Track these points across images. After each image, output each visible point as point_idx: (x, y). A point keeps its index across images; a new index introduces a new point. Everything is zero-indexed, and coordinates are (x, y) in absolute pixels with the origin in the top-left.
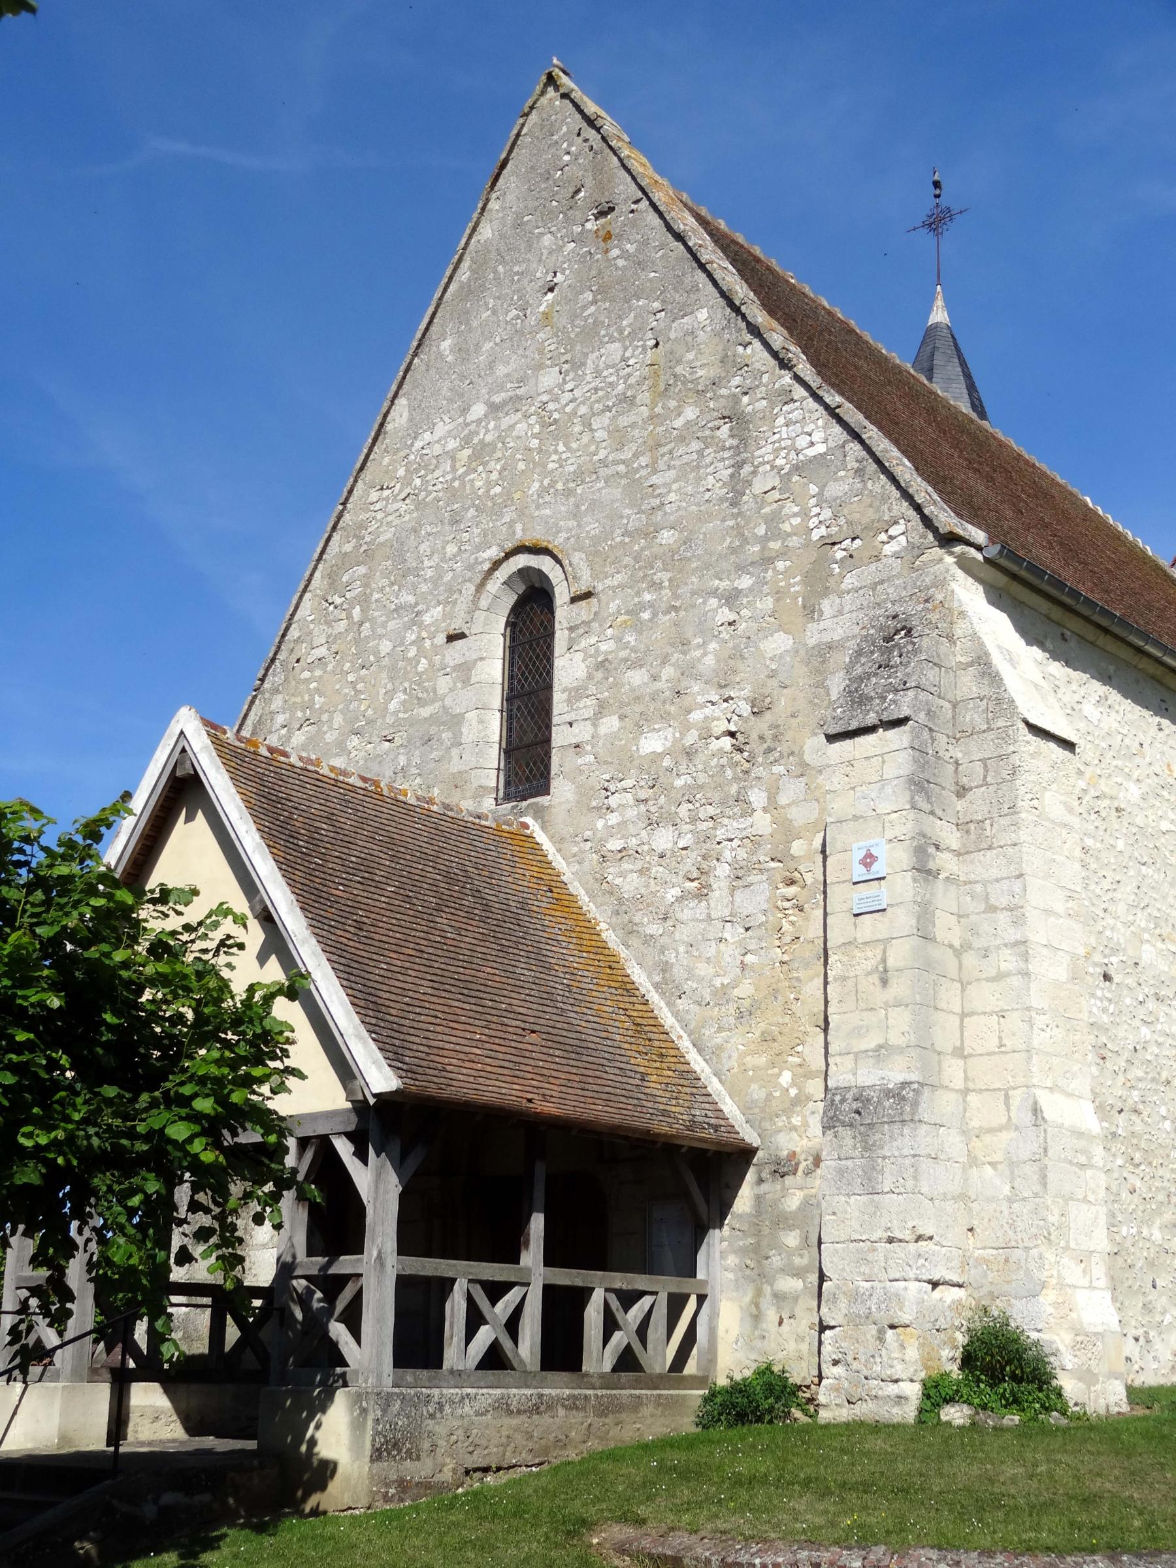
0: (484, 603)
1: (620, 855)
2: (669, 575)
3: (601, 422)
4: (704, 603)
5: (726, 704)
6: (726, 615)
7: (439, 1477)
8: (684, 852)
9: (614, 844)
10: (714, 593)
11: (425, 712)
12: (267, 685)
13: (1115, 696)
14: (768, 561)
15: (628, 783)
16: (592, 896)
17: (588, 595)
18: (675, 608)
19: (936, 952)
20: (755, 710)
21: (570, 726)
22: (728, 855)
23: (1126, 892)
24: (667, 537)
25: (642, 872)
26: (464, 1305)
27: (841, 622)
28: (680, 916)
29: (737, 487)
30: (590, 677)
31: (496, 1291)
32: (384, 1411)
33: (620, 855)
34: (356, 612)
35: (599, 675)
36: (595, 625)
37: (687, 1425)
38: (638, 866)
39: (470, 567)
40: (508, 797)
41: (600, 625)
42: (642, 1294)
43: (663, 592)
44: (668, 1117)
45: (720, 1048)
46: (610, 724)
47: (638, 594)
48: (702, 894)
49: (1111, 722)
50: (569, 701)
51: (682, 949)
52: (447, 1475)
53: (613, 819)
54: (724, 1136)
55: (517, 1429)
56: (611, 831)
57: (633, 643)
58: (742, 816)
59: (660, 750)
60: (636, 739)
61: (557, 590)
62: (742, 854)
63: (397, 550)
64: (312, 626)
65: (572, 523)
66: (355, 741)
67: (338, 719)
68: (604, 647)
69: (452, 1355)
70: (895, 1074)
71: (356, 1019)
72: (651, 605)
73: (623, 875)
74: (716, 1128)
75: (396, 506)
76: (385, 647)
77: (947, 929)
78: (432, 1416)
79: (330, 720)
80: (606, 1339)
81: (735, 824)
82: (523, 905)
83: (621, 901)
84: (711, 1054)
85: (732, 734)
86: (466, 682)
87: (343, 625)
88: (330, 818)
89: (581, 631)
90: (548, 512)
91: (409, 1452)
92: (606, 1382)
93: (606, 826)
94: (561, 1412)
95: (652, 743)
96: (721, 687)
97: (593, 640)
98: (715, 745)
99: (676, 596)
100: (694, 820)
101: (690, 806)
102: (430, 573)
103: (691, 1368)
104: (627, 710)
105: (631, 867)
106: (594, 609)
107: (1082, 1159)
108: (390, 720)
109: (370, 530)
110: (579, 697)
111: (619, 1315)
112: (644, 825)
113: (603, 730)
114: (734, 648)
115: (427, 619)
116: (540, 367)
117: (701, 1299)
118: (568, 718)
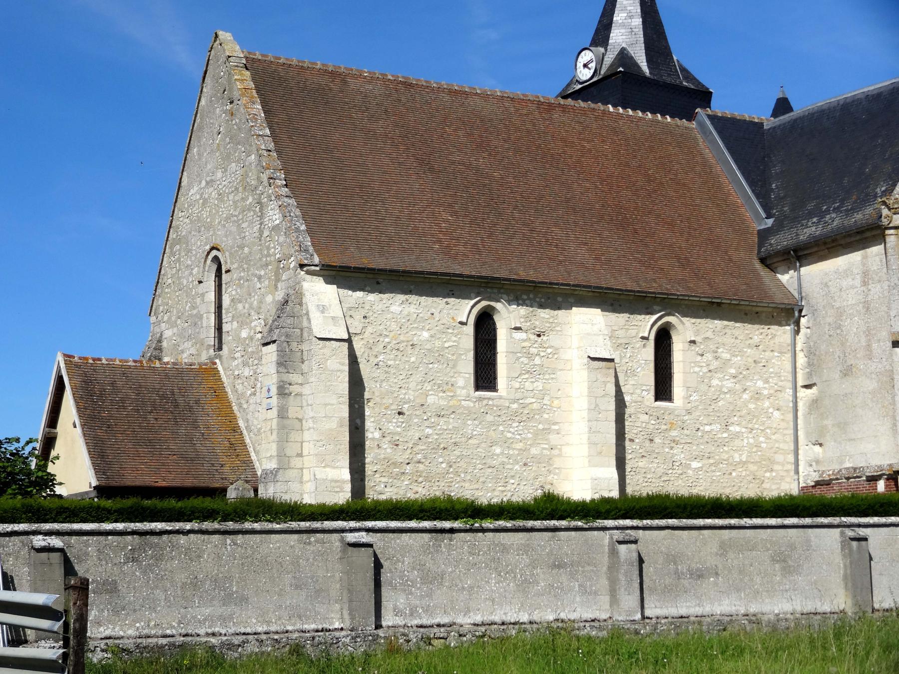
0: (207, 268)
3: (231, 197)
13: (413, 298)
14: (267, 265)
19: (286, 422)
23: (418, 377)
24: (246, 250)
27: (280, 295)
29: (261, 232)
49: (412, 309)
66: (179, 322)
70: (272, 465)
77: (292, 412)
82: (197, 402)
84: (257, 453)
88: (113, 384)
107: (338, 490)
116: (217, 168)
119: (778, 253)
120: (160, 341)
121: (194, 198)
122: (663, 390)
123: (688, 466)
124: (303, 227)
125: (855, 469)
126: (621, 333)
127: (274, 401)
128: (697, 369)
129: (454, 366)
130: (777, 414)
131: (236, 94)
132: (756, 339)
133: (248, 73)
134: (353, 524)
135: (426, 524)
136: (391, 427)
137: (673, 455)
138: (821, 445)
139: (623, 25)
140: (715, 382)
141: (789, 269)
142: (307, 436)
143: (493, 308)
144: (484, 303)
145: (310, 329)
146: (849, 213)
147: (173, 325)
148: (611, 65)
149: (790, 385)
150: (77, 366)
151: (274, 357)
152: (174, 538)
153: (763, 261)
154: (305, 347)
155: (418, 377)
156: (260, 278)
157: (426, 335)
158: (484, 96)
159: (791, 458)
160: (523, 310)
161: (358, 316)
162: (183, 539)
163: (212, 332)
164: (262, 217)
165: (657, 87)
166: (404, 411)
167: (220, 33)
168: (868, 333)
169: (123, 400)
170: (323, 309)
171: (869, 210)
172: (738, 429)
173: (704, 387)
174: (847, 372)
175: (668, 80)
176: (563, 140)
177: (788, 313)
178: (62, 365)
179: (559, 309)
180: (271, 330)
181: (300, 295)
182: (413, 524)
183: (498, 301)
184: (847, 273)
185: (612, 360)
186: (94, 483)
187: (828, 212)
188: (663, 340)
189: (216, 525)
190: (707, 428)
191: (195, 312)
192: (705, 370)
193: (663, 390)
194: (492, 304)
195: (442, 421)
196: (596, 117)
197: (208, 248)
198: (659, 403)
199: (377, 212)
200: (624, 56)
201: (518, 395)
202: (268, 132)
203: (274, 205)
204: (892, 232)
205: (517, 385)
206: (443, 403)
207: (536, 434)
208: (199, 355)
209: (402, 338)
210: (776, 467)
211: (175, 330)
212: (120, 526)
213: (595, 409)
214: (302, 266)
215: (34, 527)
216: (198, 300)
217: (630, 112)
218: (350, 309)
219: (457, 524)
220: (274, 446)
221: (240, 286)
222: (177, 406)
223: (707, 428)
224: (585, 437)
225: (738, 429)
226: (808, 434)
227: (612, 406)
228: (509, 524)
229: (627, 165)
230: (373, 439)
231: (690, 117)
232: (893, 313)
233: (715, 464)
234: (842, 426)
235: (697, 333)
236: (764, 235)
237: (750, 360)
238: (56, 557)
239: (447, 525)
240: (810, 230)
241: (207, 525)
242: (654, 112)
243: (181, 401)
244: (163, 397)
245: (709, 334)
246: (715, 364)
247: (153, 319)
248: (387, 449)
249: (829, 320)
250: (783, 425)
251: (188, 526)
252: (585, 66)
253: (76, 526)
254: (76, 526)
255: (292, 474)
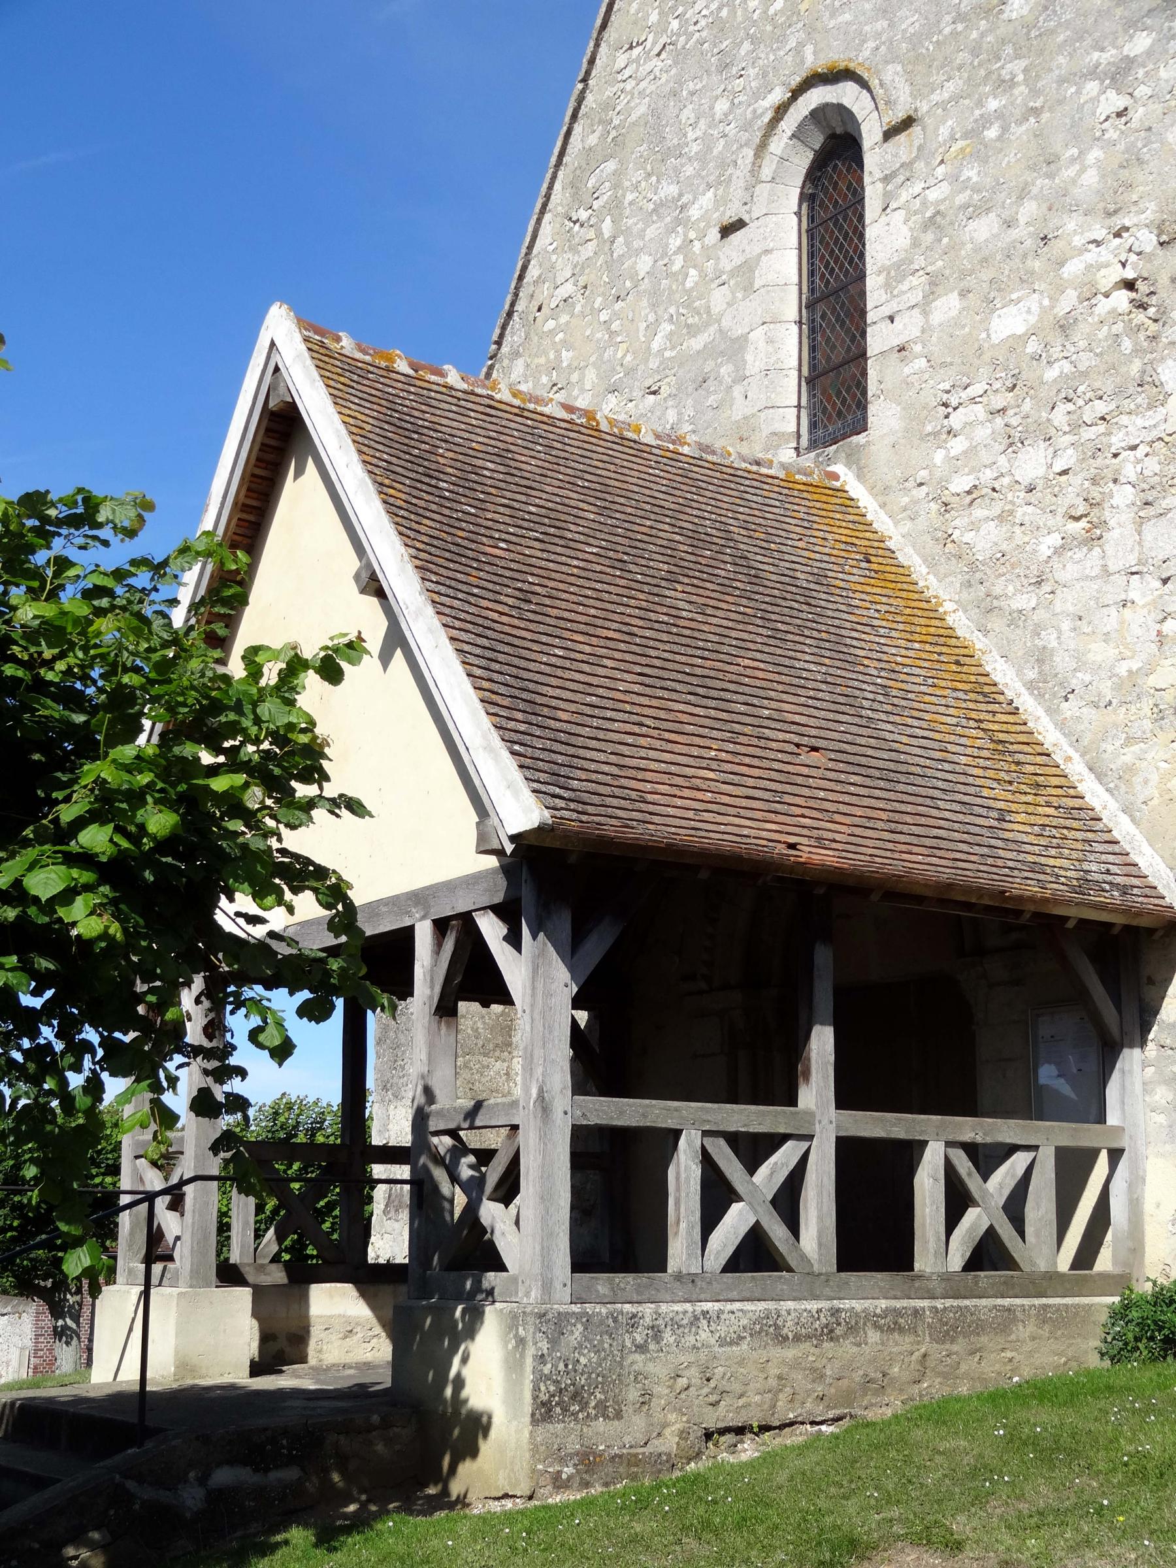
0: (767, 172)
1: (969, 498)
2: (1023, 63)
4: (1078, 92)
5: (1118, 240)
6: (1115, 101)
7: (657, 1446)
8: (1064, 478)
9: (960, 484)
10: (1093, 73)
11: (696, 343)
12: (505, 349)
15: (976, 389)
16: (932, 565)
17: (907, 123)
18: (1036, 112)
20: (1164, 238)
21: (892, 320)
22: (1130, 472)
25: (1001, 518)
26: (696, 1172)
28: (1061, 576)
30: (916, 243)
31: (754, 1149)
32: (554, 1342)
33: (969, 498)
34: (607, 227)
35: (929, 237)
36: (920, 165)
37: (1087, 1352)
38: (996, 509)
39: (746, 127)
40: (813, 445)
41: (927, 164)
42: (1013, 1149)
43: (1016, 92)
44: (1033, 866)
45: (1130, 769)
46: (948, 305)
47: (980, 103)
48: (1093, 539)
50: (888, 286)
51: (1066, 626)
52: (669, 1443)
53: (958, 445)
54: (1138, 900)
55: (796, 1365)
56: (955, 464)
57: (975, 179)
58: (1150, 407)
59: (1020, 330)
60: (987, 320)
61: (864, 129)
62: (1152, 465)
63: (655, 125)
64: (554, 257)
65: (882, 24)
67: (591, 376)
68: (933, 195)
69: (680, 1248)
71: (486, 722)
72: (999, 115)
73: (974, 527)
74: (1124, 890)
75: (648, 67)
76: (644, 264)
78: (641, 1348)
79: (581, 380)
80: (952, 1221)
81: (1140, 422)
82: (820, 578)
83: (973, 566)
85: (1130, 285)
86: (749, 289)
87: (589, 250)
89: (901, 178)
90: (847, 17)
91: (601, 1407)
92: (952, 1287)
93: (948, 459)
94: (873, 1336)
95: (1009, 323)
96: (1109, 214)
97: (918, 187)
98: (1103, 306)
99: (1035, 93)
100: (1076, 426)
101: (1070, 407)
102: (695, 148)
103: (1104, 1262)
104: (970, 282)
105: (986, 513)
106: (916, 143)
108: (654, 363)
109: (618, 108)
110: (901, 279)
111: (973, 1182)
112: (1002, 448)
113: (936, 318)
114: (1127, 151)
115: (694, 212)
117: (1115, 1155)
118: (886, 311)
150: (349, 365)
186: (520, 811)
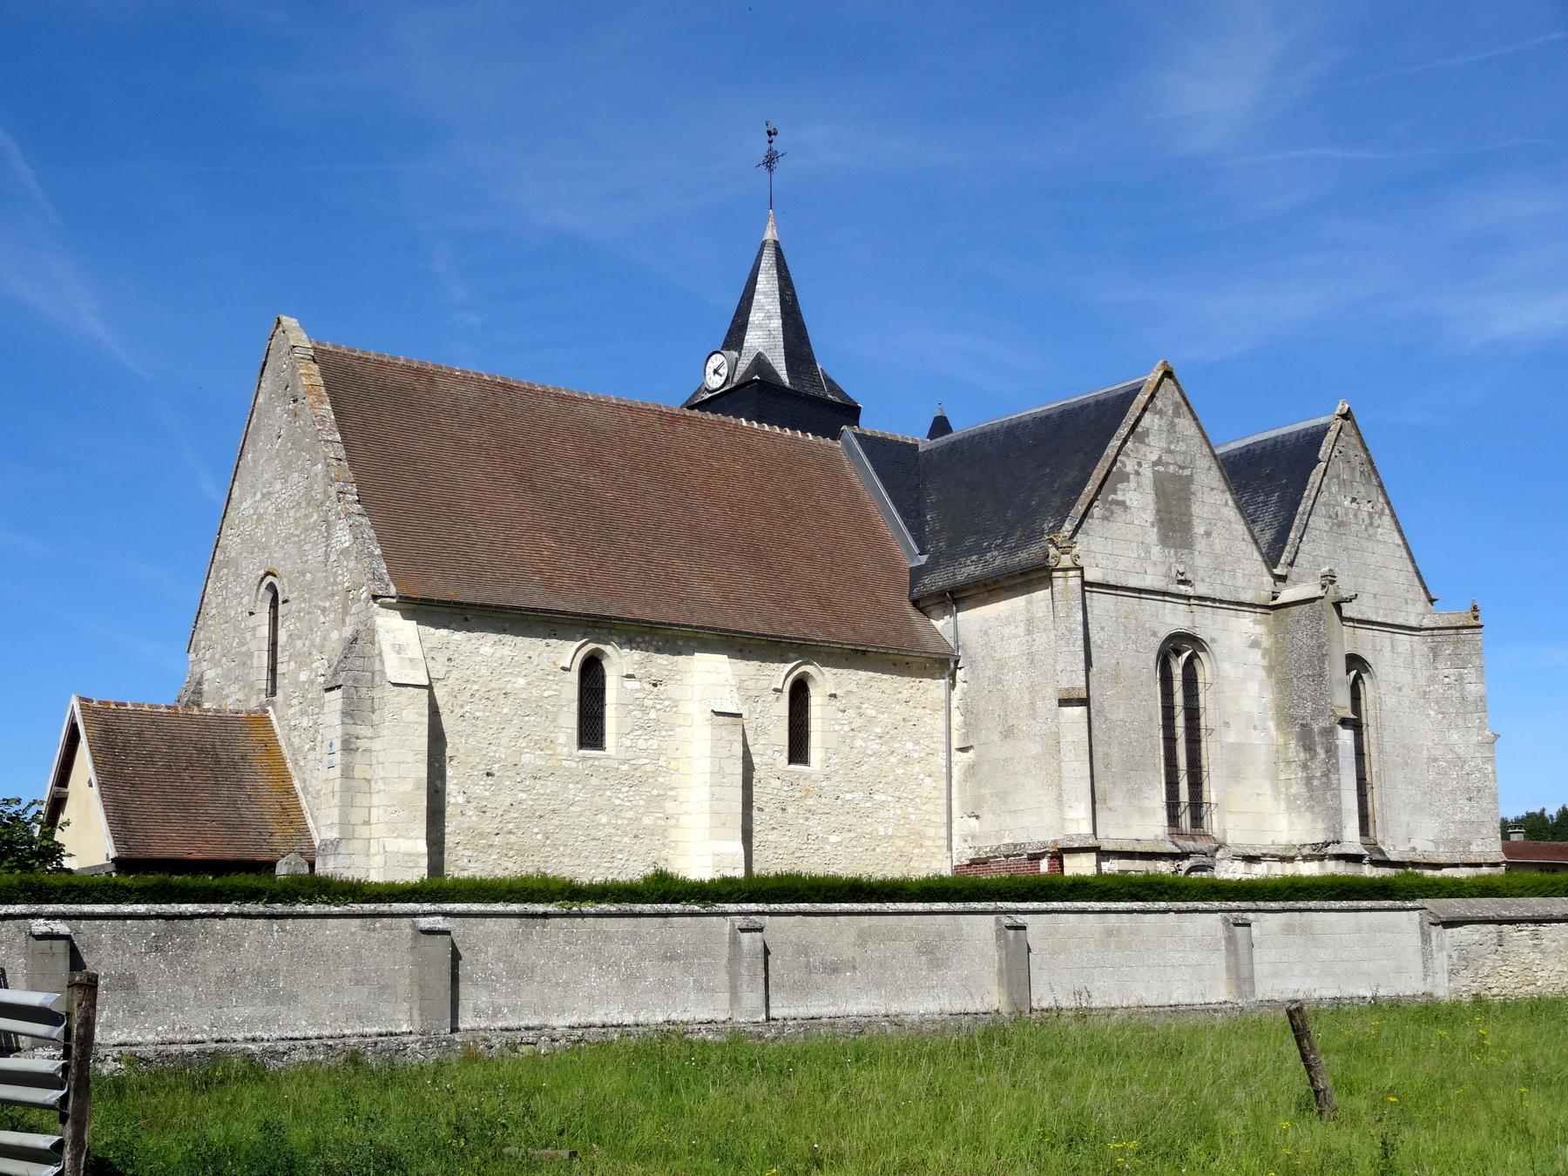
13: (508, 638)
14: (333, 595)
19: (351, 782)
23: (511, 731)
27: (348, 632)
29: (327, 555)
49: (506, 651)
70: (333, 834)
77: (358, 772)
84: (315, 819)
88: (139, 734)
119: (932, 595)
120: (199, 683)
121: (246, 513)
122: (798, 750)
123: (825, 841)
124: (378, 552)
125: (1015, 846)
126: (750, 684)
127: (338, 758)
128: (837, 728)
129: (555, 720)
130: (928, 780)
131: (301, 392)
132: (906, 694)
133: (316, 367)
134: (427, 907)
135: (515, 907)
136: (478, 790)
137: (809, 827)
138: (977, 817)
139: (760, 327)
140: (858, 743)
141: (945, 613)
142: (376, 799)
143: (602, 652)
144: (591, 646)
145: (383, 672)
146: (1012, 551)
147: (217, 664)
148: (746, 373)
149: (943, 747)
150: (96, 711)
151: (338, 706)
152: (208, 922)
153: (915, 603)
154: (376, 694)
155: (511, 731)
156: (324, 610)
157: (521, 682)
158: (597, 403)
159: (943, 832)
160: (637, 655)
161: (441, 658)
162: (219, 925)
163: (264, 674)
164: (328, 538)
165: (796, 398)
166: (494, 771)
167: (284, 318)
168: (1032, 689)
169: (151, 754)
170: (399, 649)
171: (1035, 549)
172: (883, 797)
173: (845, 749)
174: (1008, 733)
175: (811, 392)
176: (688, 457)
177: (943, 664)
178: (77, 711)
179: (679, 654)
180: (335, 673)
181: (372, 631)
182: (499, 907)
183: (608, 644)
184: (1009, 620)
185: (740, 715)
187: (988, 549)
188: (799, 693)
189: (261, 908)
190: (849, 796)
191: (243, 649)
192: (847, 728)
193: (798, 750)
194: (601, 647)
195: (538, 784)
196: (727, 432)
197: (262, 572)
198: (793, 767)
199: (467, 536)
200: (760, 363)
201: (630, 755)
202: (338, 437)
203: (343, 524)
204: (1059, 574)
205: (628, 743)
206: (540, 762)
207: (649, 801)
208: (247, 700)
209: (493, 685)
210: (926, 843)
211: (219, 670)
212: (142, 908)
213: (719, 772)
214: (375, 597)
215: (34, 908)
216: (248, 635)
217: (767, 428)
218: (432, 649)
219: (551, 908)
220: (336, 812)
221: (300, 619)
222: (218, 762)
223: (849, 796)
224: (707, 805)
225: (883, 797)
226: (963, 805)
227: (739, 769)
228: (613, 908)
229: (762, 488)
230: (456, 804)
231: (835, 435)
232: (1059, 668)
233: (858, 838)
234: (1002, 796)
235: (839, 685)
236: (917, 573)
237: (899, 718)
238: (60, 945)
239: (540, 908)
240: (969, 569)
241: (249, 907)
242: (793, 429)
243: (223, 755)
244: (201, 751)
245: (853, 687)
246: (859, 722)
247: (192, 656)
248: (472, 815)
249: (988, 673)
250: (935, 793)
251: (226, 909)
252: (716, 372)
253: (87, 908)
254: (87, 908)
255: (356, 845)
